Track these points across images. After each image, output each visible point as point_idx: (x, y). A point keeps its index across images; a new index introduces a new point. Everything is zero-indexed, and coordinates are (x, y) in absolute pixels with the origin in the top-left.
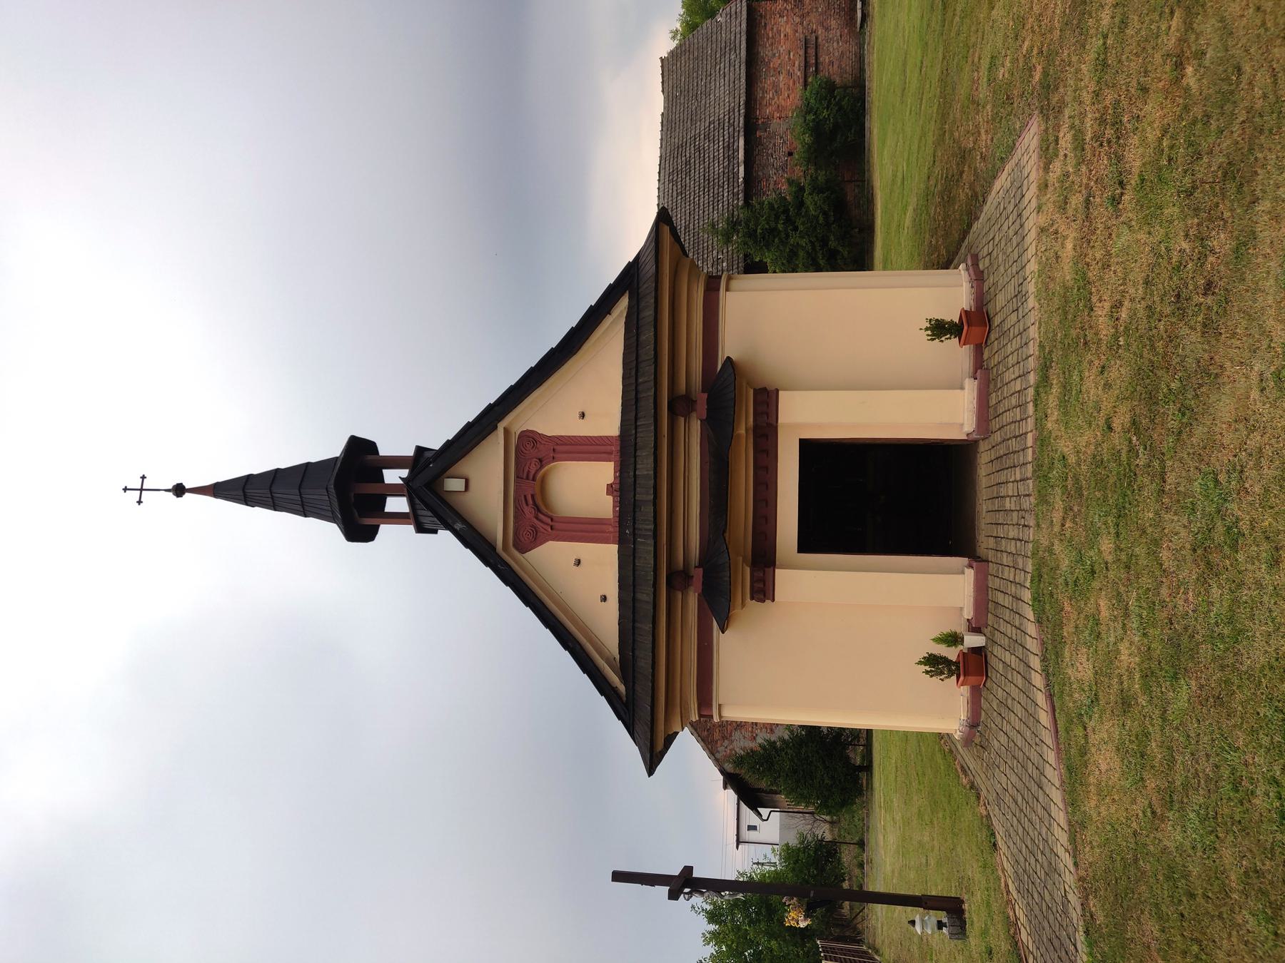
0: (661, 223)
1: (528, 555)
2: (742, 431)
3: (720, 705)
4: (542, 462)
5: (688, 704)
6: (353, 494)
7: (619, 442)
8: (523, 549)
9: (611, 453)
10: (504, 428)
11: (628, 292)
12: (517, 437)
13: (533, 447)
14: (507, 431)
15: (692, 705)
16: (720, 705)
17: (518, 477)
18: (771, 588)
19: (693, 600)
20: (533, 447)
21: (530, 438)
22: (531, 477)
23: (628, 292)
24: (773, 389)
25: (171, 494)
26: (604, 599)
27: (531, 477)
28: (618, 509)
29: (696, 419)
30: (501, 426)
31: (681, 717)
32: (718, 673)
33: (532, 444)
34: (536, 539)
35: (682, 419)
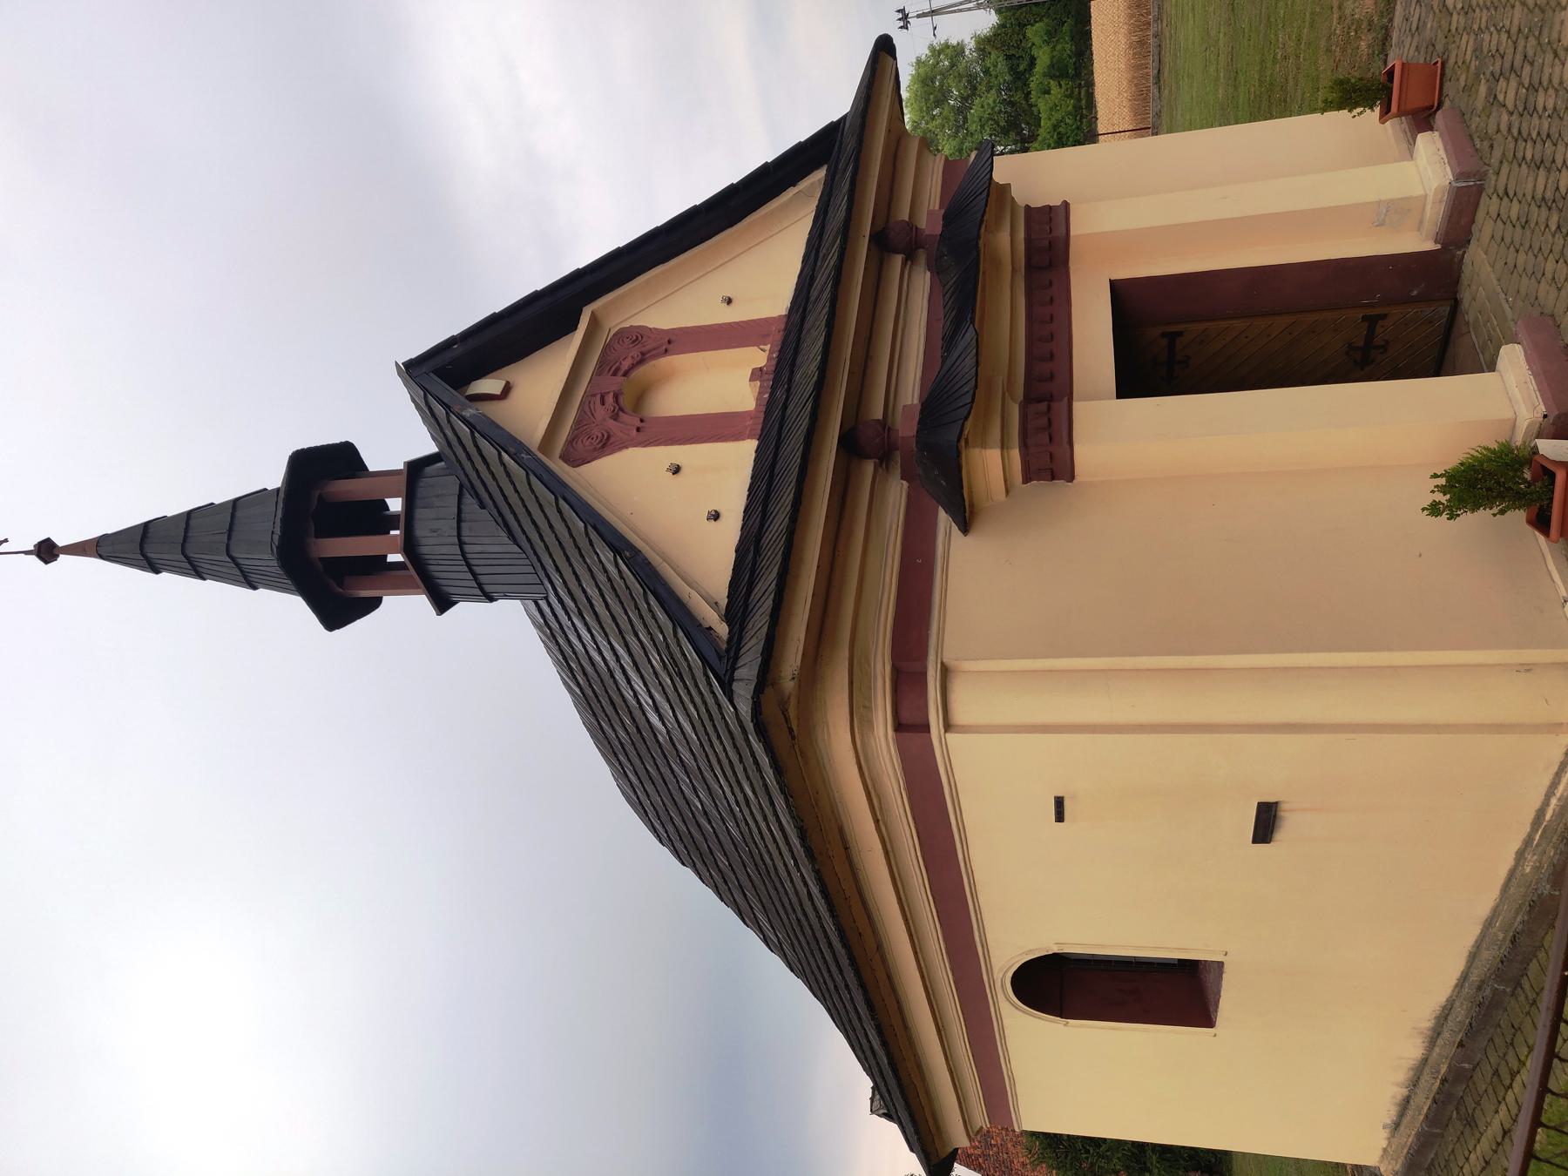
0: (883, 54)
1: (585, 469)
2: (1003, 238)
5: (869, 665)
6: (317, 493)
7: (785, 320)
8: (574, 458)
9: (768, 335)
10: (592, 312)
11: (825, 167)
12: (612, 334)
13: (633, 342)
14: (595, 322)
15: (879, 666)
16: (945, 671)
17: (599, 370)
18: (1065, 433)
19: (897, 492)
20: (633, 342)
21: (637, 336)
22: (621, 373)
23: (825, 167)
25: (34, 558)
26: (716, 516)
27: (621, 373)
28: (766, 396)
29: (922, 269)
31: (851, 683)
34: (606, 445)
35: (898, 260)
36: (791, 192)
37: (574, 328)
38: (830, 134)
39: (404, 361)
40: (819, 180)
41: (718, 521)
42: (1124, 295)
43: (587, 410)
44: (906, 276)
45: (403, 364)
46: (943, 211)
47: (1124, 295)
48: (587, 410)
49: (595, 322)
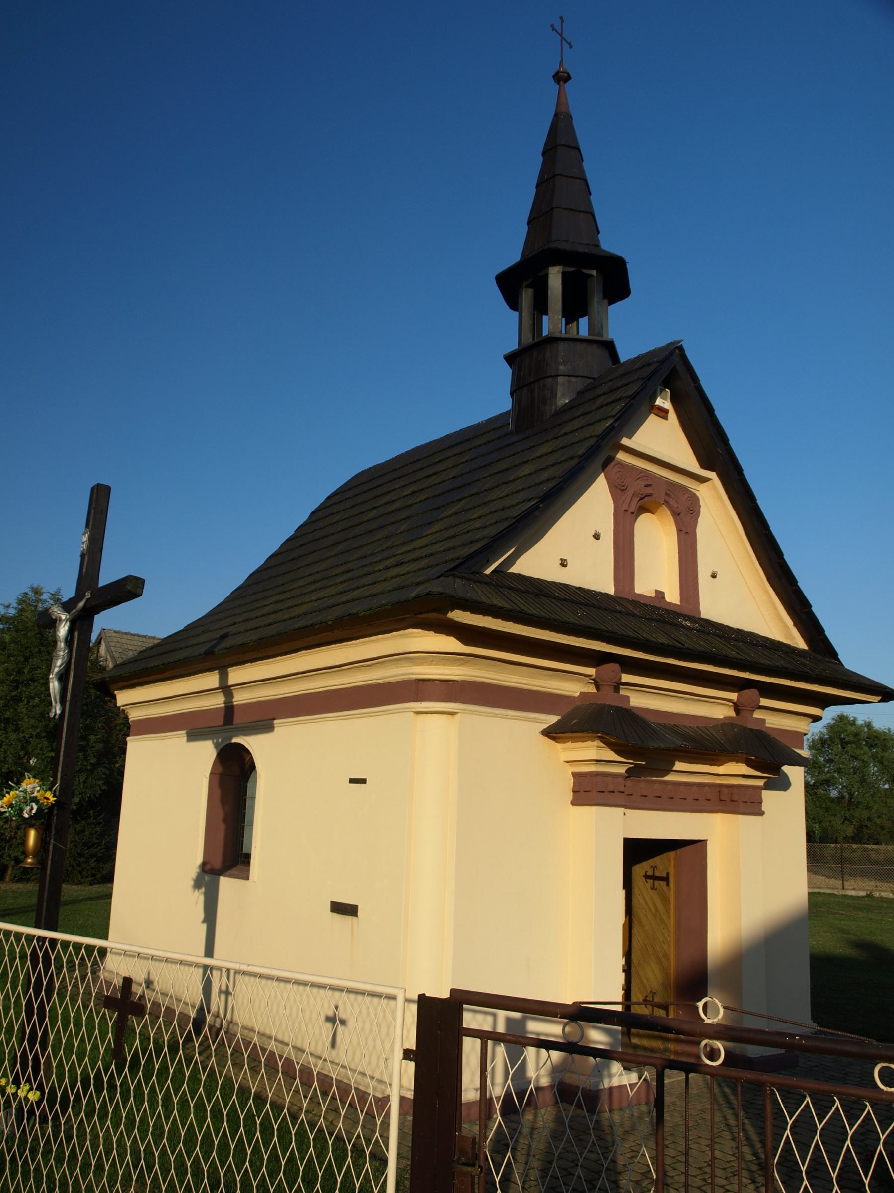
3: (452, 714)
4: (676, 515)
11: (806, 648)
16: (452, 714)
20: (689, 508)
23: (806, 648)
24: (763, 809)
30: (712, 475)
32: (495, 716)
33: (692, 509)
34: (617, 489)
36: (789, 622)
37: (704, 465)
38: (832, 653)
39: (684, 346)
40: (797, 643)
41: (560, 566)
42: (697, 846)
43: (641, 475)
44: (724, 702)
45: (682, 345)
46: (764, 730)
47: (697, 846)
48: (641, 475)
49: (703, 480)
